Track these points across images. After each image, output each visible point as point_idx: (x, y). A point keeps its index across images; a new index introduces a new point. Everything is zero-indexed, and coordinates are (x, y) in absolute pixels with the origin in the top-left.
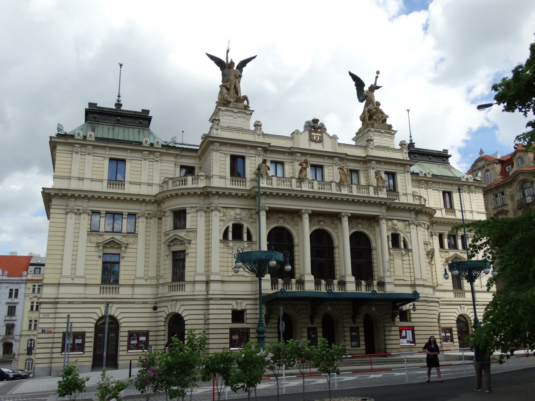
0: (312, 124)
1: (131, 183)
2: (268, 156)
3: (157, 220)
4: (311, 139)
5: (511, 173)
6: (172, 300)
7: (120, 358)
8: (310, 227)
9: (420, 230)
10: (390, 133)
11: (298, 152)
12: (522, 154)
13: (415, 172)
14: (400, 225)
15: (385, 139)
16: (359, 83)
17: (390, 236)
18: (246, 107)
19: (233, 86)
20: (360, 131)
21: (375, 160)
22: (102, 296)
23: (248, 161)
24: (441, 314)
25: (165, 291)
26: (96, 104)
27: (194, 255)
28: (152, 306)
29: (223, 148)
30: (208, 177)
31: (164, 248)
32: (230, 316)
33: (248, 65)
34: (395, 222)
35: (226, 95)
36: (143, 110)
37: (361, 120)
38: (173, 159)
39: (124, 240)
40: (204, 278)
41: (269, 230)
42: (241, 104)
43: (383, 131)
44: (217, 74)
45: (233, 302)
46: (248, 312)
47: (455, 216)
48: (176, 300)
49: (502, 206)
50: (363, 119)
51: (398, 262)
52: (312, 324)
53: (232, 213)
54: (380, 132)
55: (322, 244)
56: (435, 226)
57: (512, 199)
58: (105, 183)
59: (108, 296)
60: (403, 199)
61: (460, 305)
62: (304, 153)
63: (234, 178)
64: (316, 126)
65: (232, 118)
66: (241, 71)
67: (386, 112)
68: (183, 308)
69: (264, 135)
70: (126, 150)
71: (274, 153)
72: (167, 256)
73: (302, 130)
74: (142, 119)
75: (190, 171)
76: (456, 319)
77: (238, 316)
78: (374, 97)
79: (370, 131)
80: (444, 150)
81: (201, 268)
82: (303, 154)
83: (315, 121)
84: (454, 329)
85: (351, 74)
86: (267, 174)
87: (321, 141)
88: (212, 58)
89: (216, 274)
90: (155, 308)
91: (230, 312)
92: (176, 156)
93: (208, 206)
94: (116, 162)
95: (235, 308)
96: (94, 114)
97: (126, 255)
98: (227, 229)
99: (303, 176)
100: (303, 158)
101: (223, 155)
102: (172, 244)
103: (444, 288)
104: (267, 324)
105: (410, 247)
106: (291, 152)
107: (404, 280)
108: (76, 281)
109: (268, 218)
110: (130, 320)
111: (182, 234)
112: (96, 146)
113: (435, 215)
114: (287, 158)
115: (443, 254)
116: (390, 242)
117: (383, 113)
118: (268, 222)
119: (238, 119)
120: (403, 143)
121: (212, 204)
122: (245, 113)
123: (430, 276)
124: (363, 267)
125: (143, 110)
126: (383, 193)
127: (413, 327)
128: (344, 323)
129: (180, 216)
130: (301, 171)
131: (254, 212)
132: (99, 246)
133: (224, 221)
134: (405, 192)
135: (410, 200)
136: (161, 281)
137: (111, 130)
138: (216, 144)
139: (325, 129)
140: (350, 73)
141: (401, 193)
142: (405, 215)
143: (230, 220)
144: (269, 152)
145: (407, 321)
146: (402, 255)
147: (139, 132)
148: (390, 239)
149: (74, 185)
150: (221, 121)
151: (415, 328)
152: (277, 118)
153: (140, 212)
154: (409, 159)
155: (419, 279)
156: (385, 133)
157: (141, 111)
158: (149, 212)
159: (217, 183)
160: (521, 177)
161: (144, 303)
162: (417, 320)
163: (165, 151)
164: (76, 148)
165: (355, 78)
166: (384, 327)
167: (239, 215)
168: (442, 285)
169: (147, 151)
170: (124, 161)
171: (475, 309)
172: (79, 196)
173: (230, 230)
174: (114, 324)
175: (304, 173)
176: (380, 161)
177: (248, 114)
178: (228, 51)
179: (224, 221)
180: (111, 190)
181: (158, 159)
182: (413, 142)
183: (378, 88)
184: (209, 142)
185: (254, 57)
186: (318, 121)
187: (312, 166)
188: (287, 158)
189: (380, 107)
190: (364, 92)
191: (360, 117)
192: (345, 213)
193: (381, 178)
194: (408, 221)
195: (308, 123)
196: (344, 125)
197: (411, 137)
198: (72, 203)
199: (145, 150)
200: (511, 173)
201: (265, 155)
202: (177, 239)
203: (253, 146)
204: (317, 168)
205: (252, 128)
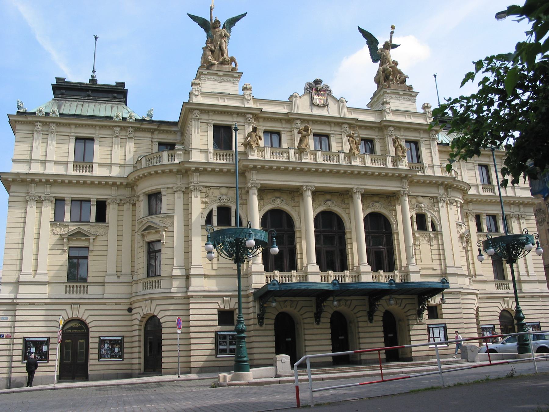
1: (101, 165)
2: (261, 124)
3: (131, 206)
4: (313, 104)
7: (90, 368)
8: (314, 208)
9: (451, 208)
10: (411, 95)
11: (298, 119)
13: (444, 142)
14: (425, 205)
15: (404, 102)
16: (371, 41)
17: (415, 216)
18: (234, 70)
19: (217, 48)
20: (375, 94)
21: (393, 126)
22: (68, 296)
24: (480, 310)
26: (64, 79)
27: (170, 245)
28: (127, 307)
29: (205, 117)
30: (187, 152)
31: (138, 236)
32: (216, 317)
33: (237, 24)
34: (421, 199)
35: (210, 57)
36: (116, 83)
37: (376, 82)
38: (149, 135)
39: (92, 231)
41: (263, 213)
42: (227, 66)
43: (401, 93)
44: (201, 35)
48: (151, 299)
50: (377, 80)
51: (425, 247)
54: (398, 94)
55: (331, 231)
56: (471, 207)
58: (70, 166)
59: (74, 296)
60: (428, 172)
61: (503, 298)
62: (306, 120)
63: (218, 152)
64: (319, 88)
65: (216, 83)
66: (230, 30)
67: (405, 73)
69: (255, 100)
70: (94, 126)
71: (273, 126)
73: (301, 92)
74: (118, 93)
75: (171, 146)
78: (389, 55)
79: (385, 93)
82: (303, 121)
83: (318, 82)
84: (496, 327)
85: (361, 30)
86: (257, 144)
88: (194, 18)
90: (130, 310)
91: (216, 311)
92: (153, 131)
93: (187, 186)
94: (83, 141)
95: (222, 306)
96: (62, 89)
97: (96, 248)
99: (303, 146)
101: (204, 125)
102: (145, 233)
103: (483, 278)
106: (289, 119)
107: (433, 269)
108: (38, 279)
109: (260, 198)
110: (101, 324)
111: (156, 220)
112: (60, 123)
113: (469, 192)
116: (415, 224)
117: (400, 73)
118: (262, 202)
119: (224, 84)
120: (426, 105)
121: (191, 183)
122: (233, 76)
123: (465, 263)
124: (382, 254)
125: (116, 83)
126: (404, 164)
127: (445, 324)
128: (358, 322)
129: (154, 197)
130: (301, 141)
132: (63, 239)
134: (430, 163)
136: (135, 278)
137: (80, 106)
138: (195, 111)
142: (432, 192)
143: (213, 202)
144: (261, 120)
145: (437, 318)
146: (430, 239)
147: (112, 107)
148: (415, 219)
149: (36, 169)
151: (448, 326)
152: (269, 78)
153: (110, 197)
155: (451, 267)
156: (404, 94)
157: (115, 84)
158: (121, 198)
159: (197, 157)
163: (139, 126)
164: (37, 127)
168: (481, 275)
169: (119, 126)
170: (92, 139)
172: (40, 181)
173: (215, 213)
174: (83, 329)
175: (305, 142)
176: (399, 126)
177: (235, 77)
178: (211, 9)
180: (78, 173)
181: (131, 136)
183: (395, 46)
184: (189, 110)
185: (245, 15)
187: (315, 135)
188: (284, 126)
189: (398, 67)
191: (375, 78)
192: (357, 189)
193: (401, 146)
194: (436, 198)
195: (310, 85)
198: (33, 190)
199: (116, 126)
201: (257, 124)
202: (151, 226)
203: (242, 113)
204: (323, 138)
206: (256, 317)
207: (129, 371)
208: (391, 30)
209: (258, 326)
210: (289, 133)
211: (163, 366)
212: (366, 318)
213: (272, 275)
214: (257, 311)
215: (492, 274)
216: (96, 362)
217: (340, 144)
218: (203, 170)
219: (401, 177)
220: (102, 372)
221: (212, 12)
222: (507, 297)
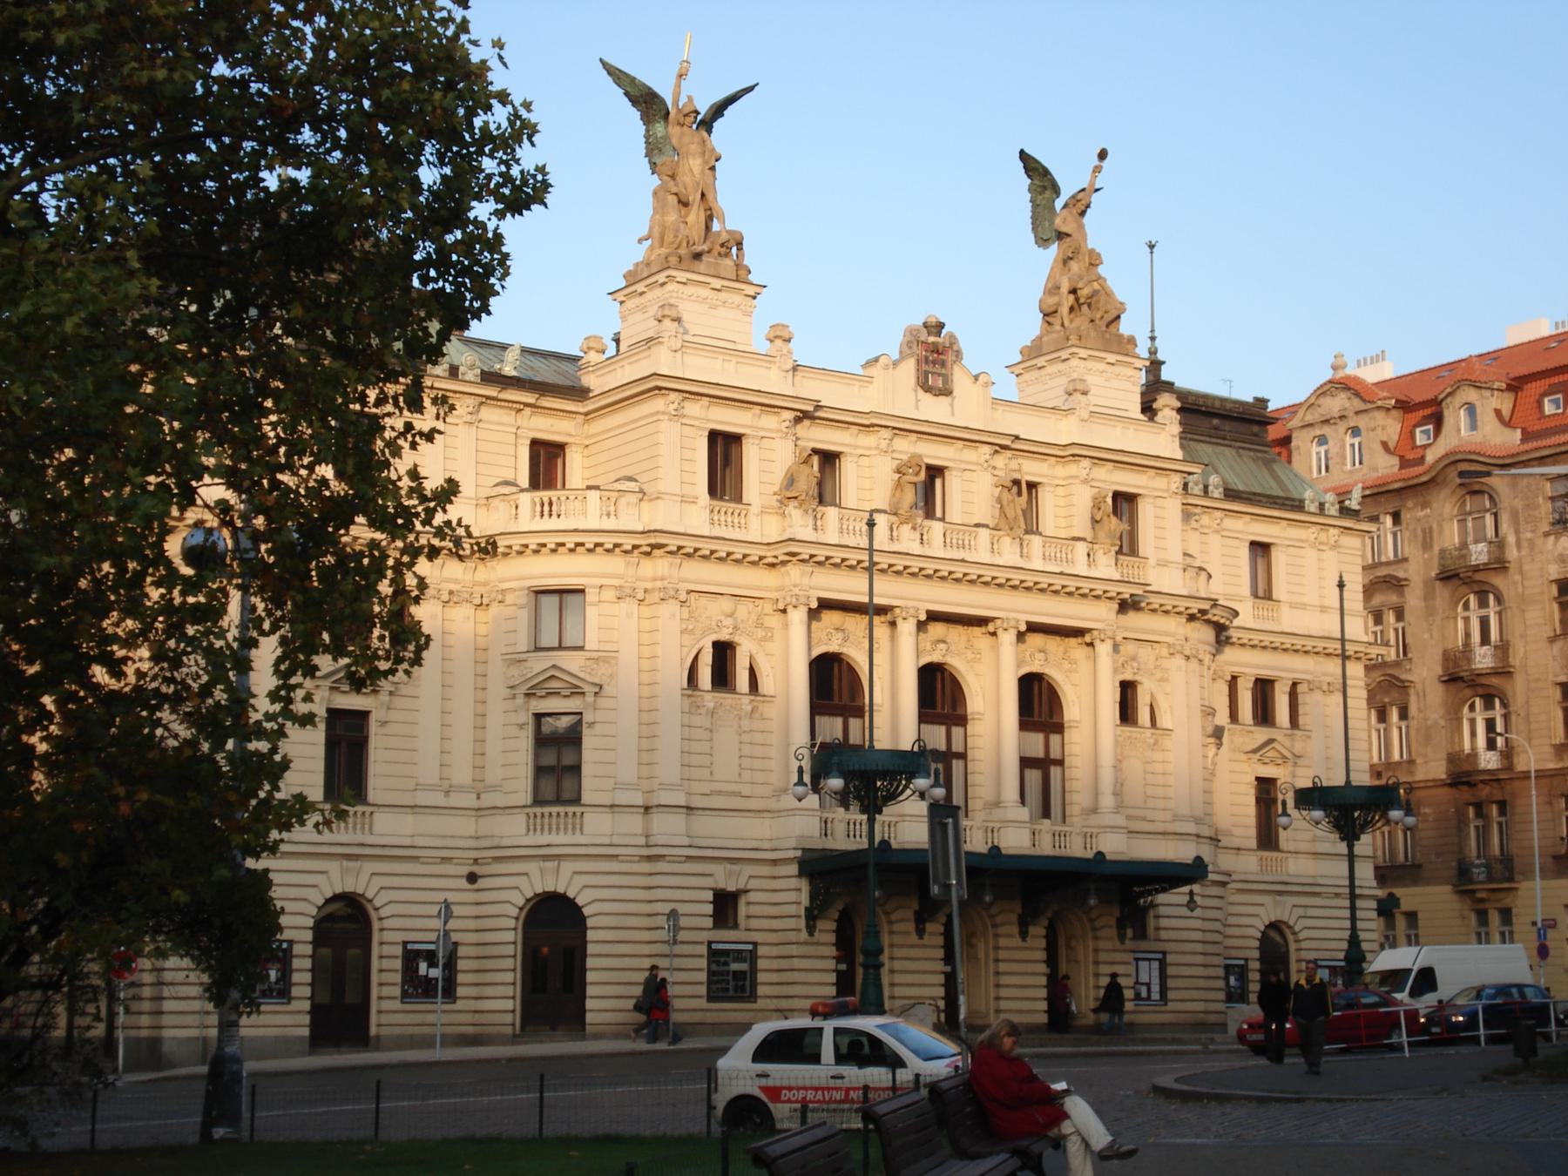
0: (924, 336)
5: (1431, 457)
6: (545, 858)
18: (741, 274)
25: (513, 830)
28: (465, 870)
29: (694, 408)
32: (709, 909)
40: (638, 799)
43: (1112, 358)
45: (718, 870)
46: (752, 897)
52: (921, 937)
59: (344, 838)
68: (581, 880)
72: (521, 726)
73: (895, 356)
76: (1259, 935)
77: (725, 905)
80: (1257, 399)
87: (946, 392)
89: (671, 787)
90: (472, 878)
91: (710, 896)
95: (721, 885)
97: (393, 715)
100: (907, 447)
104: (811, 934)
105: (1164, 720)
114: (852, 441)
131: (769, 607)
133: (692, 632)
140: (1023, 156)
141: (1152, 562)
150: (685, 318)
154: (1179, 455)
158: (453, 587)
161: (444, 860)
166: (1096, 951)
167: (731, 615)
171: (1353, 908)
179: (692, 632)
182: (1160, 356)
185: (751, 89)
186: (941, 326)
195: (911, 332)
197: (1153, 339)
200: (1431, 457)
203: (767, 405)
206: (803, 912)
207: (470, 1030)
208: (1096, 162)
209: (804, 935)
211: (589, 1018)
212: (1015, 930)
213: (831, 816)
214: (805, 899)
216: (397, 1005)
220: (410, 1030)
222: (1280, 893)
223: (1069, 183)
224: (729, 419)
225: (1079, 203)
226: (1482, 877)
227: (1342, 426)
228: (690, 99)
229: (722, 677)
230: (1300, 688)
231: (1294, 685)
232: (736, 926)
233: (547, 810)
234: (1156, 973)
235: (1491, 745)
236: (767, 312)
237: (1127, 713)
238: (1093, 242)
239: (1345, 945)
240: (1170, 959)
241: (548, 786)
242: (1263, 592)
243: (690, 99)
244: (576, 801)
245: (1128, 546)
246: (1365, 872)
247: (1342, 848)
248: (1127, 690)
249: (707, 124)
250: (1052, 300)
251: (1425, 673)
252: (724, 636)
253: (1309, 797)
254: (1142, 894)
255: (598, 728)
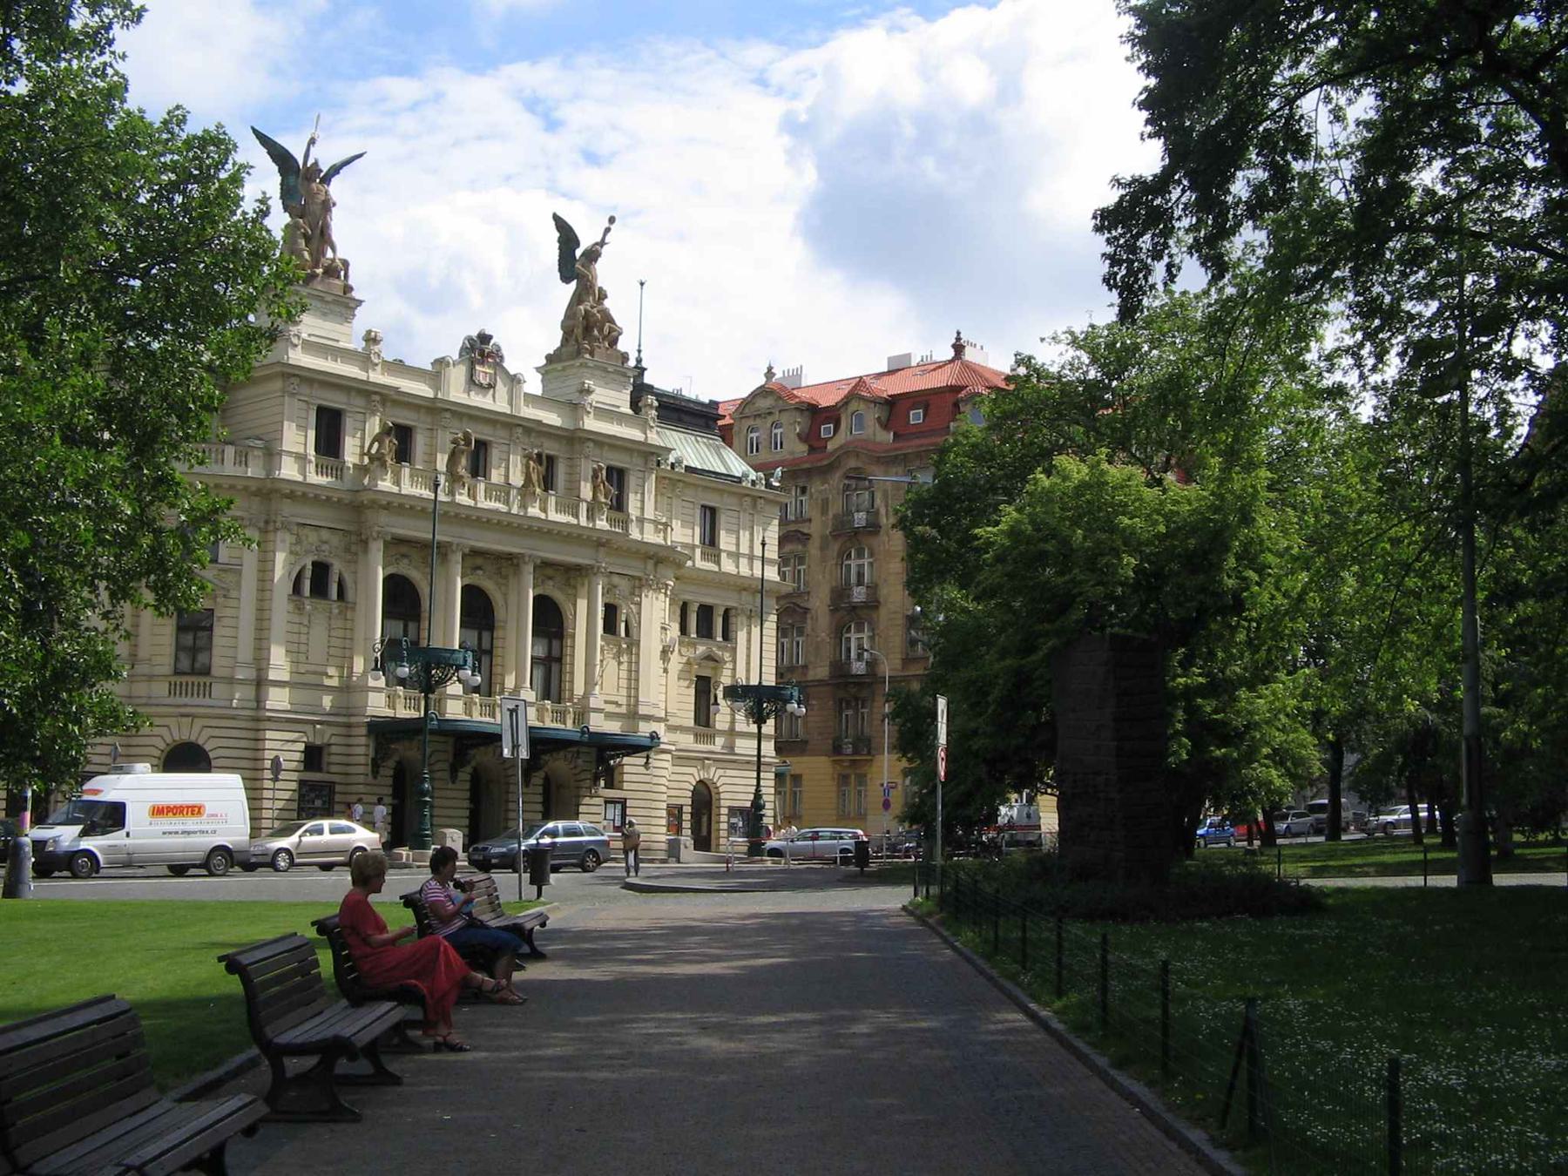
4: (472, 383)
12: (862, 406)
16: (567, 237)
23: (349, 423)
29: (305, 389)
46: (334, 749)
47: (718, 563)
48: (194, 716)
49: (795, 522)
53: (312, 537)
57: (824, 509)
73: (456, 357)
81: (245, 652)
98: (303, 568)
101: (304, 406)
106: (436, 409)
115: (684, 650)
135: (651, 536)
138: (293, 380)
139: (502, 358)
140: (556, 218)
143: (307, 552)
159: (288, 470)
160: (852, 463)
162: (633, 787)
165: (562, 225)
173: (308, 573)
178: (312, 142)
182: (644, 364)
185: (360, 156)
186: (490, 337)
190: (575, 261)
194: (640, 579)
196: (530, 337)
200: (830, 446)
205: (358, 345)
209: (370, 779)
210: (428, 433)
214: (371, 753)
215: (692, 714)
217: (510, 469)
218: (299, 494)
219: (600, 543)
221: (312, 149)
223: (586, 240)
224: (334, 400)
225: (593, 255)
226: (849, 751)
227: (770, 420)
228: (316, 163)
229: (319, 589)
230: (733, 612)
231: (727, 611)
232: (320, 770)
233: (184, 679)
234: (618, 812)
235: (860, 657)
236: (364, 320)
237: (610, 627)
238: (600, 283)
239: (751, 797)
240: (629, 803)
241: (185, 664)
242: (710, 540)
243: (316, 163)
244: (206, 671)
245: (619, 505)
246: (768, 748)
247: (754, 728)
248: (611, 611)
249: (326, 179)
250: (570, 323)
251: (819, 603)
252: (322, 558)
253: (733, 692)
254: (613, 757)
255: (226, 622)
